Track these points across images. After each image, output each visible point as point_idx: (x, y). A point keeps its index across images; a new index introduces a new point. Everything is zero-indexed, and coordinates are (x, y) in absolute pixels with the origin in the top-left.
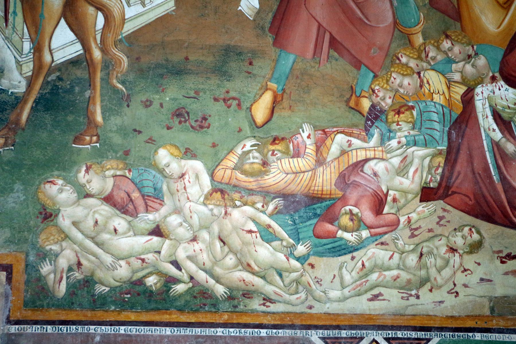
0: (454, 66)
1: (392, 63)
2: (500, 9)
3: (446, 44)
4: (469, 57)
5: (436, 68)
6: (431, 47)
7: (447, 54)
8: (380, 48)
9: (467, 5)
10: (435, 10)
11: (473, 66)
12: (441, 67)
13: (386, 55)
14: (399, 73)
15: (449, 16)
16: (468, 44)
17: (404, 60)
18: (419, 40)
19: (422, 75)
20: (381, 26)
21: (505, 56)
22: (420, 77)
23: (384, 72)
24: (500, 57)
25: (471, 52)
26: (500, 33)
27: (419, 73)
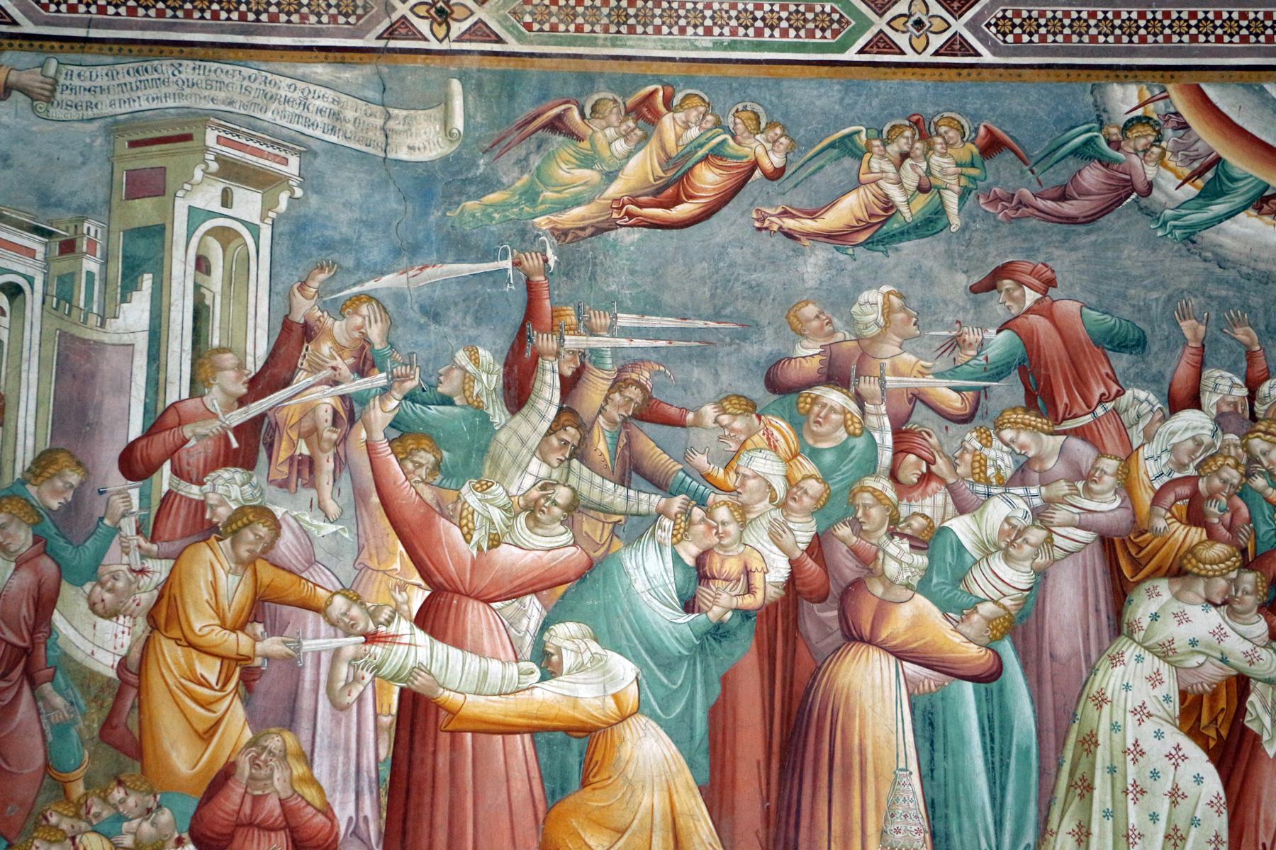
0: (125, 825)
1: (37, 825)
2: (199, 743)
3: (118, 794)
4: (149, 811)
5: (99, 829)
6: (95, 799)
7: (117, 808)
8: (21, 805)
9: (153, 738)
10: (105, 745)
11: (153, 824)
12: (105, 828)
13: (29, 814)
14: (45, 839)
15: (126, 753)
16: (148, 793)
17: (54, 820)
18: (78, 789)
19: (77, 840)
20: (25, 771)
21: (199, 808)
22: (74, 843)
23: (23, 839)
24: (192, 810)
25: (152, 804)
26: (195, 775)
27: (73, 839)
